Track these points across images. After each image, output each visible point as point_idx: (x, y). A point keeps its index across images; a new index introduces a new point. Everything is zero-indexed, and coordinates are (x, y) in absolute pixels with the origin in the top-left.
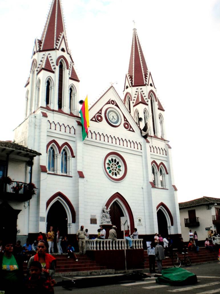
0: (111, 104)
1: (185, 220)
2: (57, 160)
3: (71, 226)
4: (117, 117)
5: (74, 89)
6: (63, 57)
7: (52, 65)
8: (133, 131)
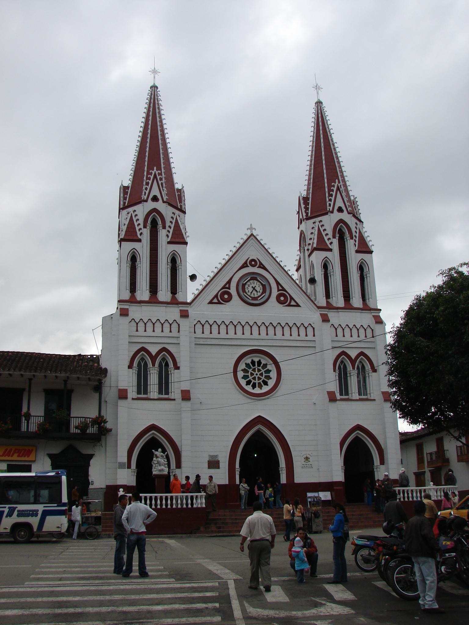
3: (378, 470)
7: (326, 238)
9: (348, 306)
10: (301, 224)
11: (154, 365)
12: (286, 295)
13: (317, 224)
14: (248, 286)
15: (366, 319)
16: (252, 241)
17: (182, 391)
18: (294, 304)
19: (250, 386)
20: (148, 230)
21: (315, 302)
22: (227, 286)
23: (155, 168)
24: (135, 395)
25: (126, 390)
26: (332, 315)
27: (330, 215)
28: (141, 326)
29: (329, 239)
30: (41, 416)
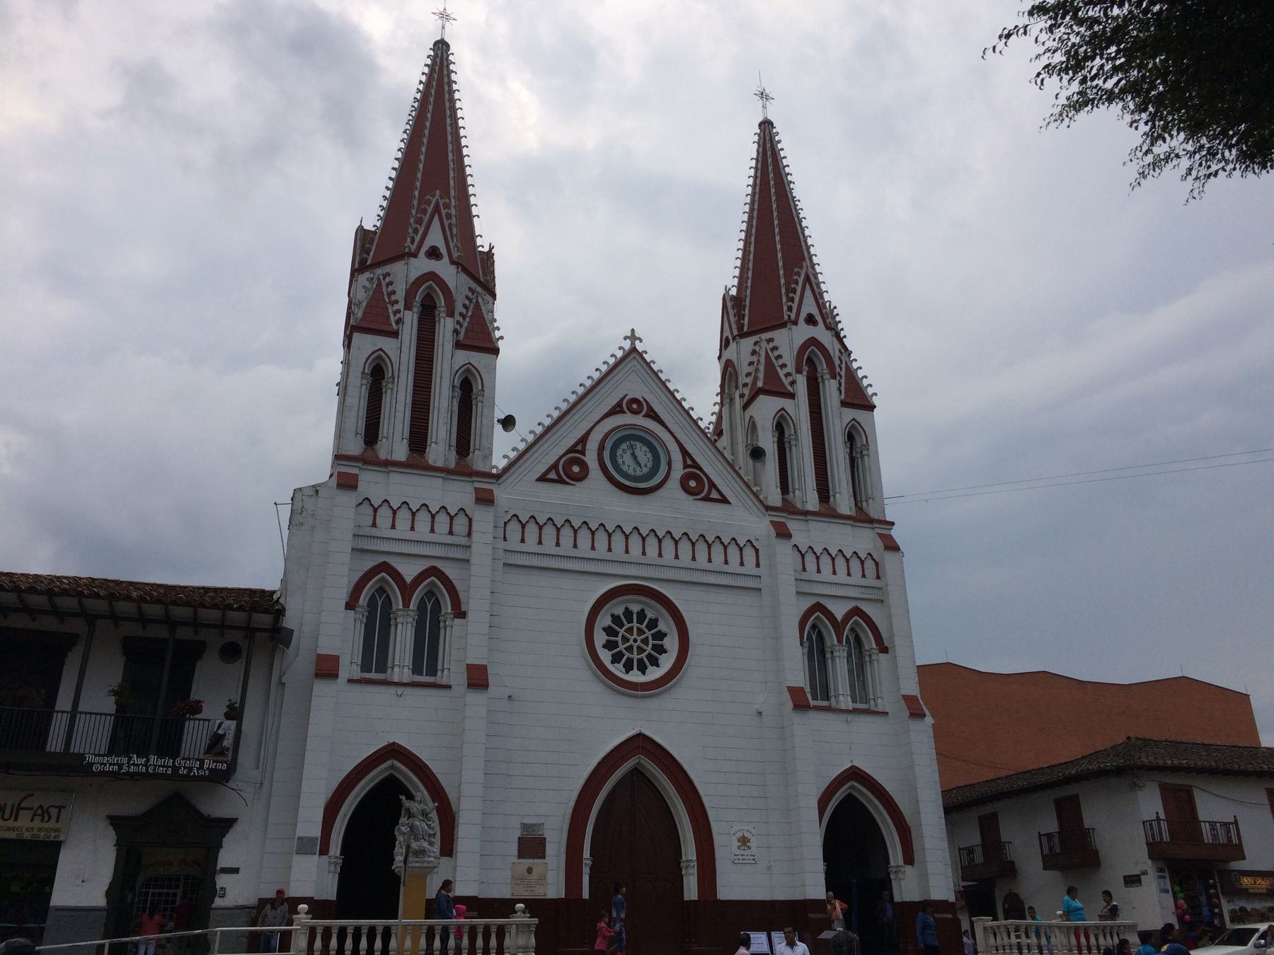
0: (629, 414)
1: (1044, 839)
2: (874, 667)
4: (651, 458)
5: (789, 426)
6: (813, 341)
7: (782, 373)
8: (724, 500)
9: (827, 512)
10: (725, 350)
11: (406, 604)
12: (698, 475)
13: (764, 344)
14: (623, 452)
15: (862, 540)
16: (633, 363)
17: (471, 668)
18: (718, 497)
19: (620, 666)
20: (415, 315)
21: (761, 497)
22: (579, 448)
23: (438, 193)
24: (357, 673)
25: (335, 659)
26: (793, 525)
27: (791, 329)
28: (384, 515)
29: (788, 375)
30: (106, 715)
